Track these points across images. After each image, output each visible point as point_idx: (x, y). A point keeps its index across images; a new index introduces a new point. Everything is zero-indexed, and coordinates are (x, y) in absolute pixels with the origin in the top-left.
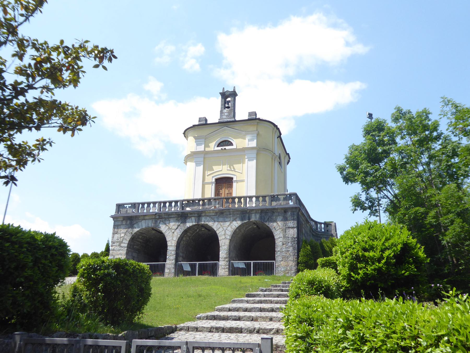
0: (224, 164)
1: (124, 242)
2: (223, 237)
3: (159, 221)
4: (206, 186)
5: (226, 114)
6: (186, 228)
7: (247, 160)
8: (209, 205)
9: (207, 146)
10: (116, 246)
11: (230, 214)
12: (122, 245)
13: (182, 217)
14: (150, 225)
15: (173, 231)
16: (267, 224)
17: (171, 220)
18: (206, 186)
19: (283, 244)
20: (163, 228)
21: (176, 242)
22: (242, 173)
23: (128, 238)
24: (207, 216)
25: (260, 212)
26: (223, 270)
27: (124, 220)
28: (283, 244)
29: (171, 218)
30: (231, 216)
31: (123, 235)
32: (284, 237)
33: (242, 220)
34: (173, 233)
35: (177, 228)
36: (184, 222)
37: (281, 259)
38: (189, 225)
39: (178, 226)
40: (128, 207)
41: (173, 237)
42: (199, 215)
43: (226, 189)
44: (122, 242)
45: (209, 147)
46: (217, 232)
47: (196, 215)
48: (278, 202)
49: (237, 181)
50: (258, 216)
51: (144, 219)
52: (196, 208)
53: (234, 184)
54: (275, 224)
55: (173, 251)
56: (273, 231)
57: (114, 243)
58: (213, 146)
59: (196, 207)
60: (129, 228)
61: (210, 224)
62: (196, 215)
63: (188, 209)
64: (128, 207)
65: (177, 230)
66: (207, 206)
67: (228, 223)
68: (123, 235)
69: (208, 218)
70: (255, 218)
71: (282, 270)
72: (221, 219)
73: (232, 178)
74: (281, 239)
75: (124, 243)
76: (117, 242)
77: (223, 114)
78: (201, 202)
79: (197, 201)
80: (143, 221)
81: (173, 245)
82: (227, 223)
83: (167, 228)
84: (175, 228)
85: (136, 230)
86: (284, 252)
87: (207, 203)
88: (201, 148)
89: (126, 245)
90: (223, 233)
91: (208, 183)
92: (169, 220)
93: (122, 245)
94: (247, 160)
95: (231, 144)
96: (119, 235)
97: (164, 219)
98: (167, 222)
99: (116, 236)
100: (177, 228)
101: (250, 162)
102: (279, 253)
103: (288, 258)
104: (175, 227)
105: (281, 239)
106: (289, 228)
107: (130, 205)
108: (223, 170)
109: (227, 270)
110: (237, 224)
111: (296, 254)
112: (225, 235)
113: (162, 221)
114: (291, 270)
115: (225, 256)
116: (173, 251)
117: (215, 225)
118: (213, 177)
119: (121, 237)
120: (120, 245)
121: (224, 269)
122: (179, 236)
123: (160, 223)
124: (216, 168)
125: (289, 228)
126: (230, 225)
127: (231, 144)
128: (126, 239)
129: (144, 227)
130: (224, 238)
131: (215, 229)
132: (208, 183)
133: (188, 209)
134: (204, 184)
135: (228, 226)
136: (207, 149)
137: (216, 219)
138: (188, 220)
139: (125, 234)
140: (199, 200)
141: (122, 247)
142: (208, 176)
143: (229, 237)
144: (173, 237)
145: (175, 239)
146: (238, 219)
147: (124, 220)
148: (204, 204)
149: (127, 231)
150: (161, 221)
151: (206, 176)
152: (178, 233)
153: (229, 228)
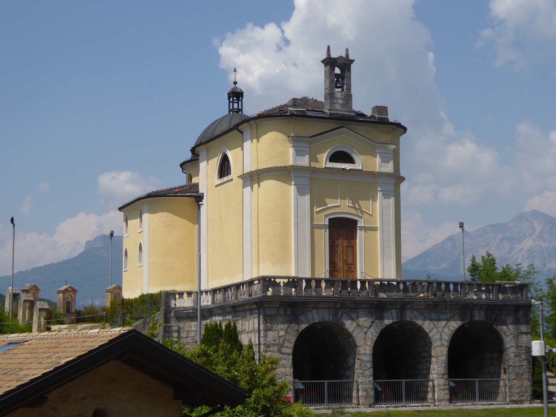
0: (343, 198)
1: (286, 344)
2: (439, 343)
3: (340, 313)
4: (316, 231)
5: (340, 101)
6: (385, 326)
7: (379, 194)
8: (413, 292)
9: (313, 159)
10: (273, 351)
11: (446, 309)
12: (284, 350)
13: (377, 309)
14: (327, 318)
15: (365, 330)
16: (495, 326)
17: (361, 312)
18: (316, 231)
19: (516, 356)
20: (349, 325)
21: (372, 348)
22: (371, 215)
23: (293, 338)
24: (415, 309)
25: (485, 308)
26: (443, 392)
27: (281, 306)
28: (516, 356)
29: (360, 308)
30: (448, 311)
31: (282, 333)
32: (517, 346)
33: (462, 319)
34: (366, 333)
35: (371, 326)
36: (381, 318)
37: (514, 377)
38: (387, 322)
39: (373, 322)
40: (282, 284)
41: (365, 339)
42: (402, 306)
43: (345, 241)
44: (282, 346)
45: (317, 161)
46: (431, 335)
47: (398, 307)
48: (505, 295)
49: (366, 229)
50: (483, 314)
51: (316, 308)
52: (395, 295)
53: (360, 234)
54: (505, 327)
55: (369, 362)
56: (503, 336)
57: (269, 347)
58: (323, 161)
59: (395, 293)
60: (291, 322)
61: (420, 322)
62: (398, 307)
63: (382, 295)
64: (282, 284)
65: (372, 330)
66: (411, 293)
67: (443, 323)
68: (282, 333)
69: (415, 312)
70: (479, 316)
71: (517, 391)
72: (434, 315)
73: (355, 222)
74: (512, 350)
75: (287, 347)
76: (275, 345)
77: (335, 101)
78: (401, 286)
79: (395, 283)
80: (314, 312)
81: (368, 352)
82: (442, 322)
83: (355, 324)
84: (368, 325)
85: (303, 326)
86: (517, 368)
87: (410, 288)
88: (305, 161)
89: (290, 351)
90: (438, 336)
91: (320, 227)
92: (357, 312)
93: (284, 350)
94: (379, 194)
95: (352, 161)
96: (276, 333)
97: (348, 310)
98: (354, 316)
99: (271, 334)
100: (371, 326)
101: (386, 201)
102: (511, 368)
103: (522, 375)
104: (367, 324)
105: (512, 350)
106: (522, 333)
107: (286, 281)
108: (341, 207)
109: (447, 392)
110: (455, 325)
111: (531, 371)
112: (441, 339)
113: (346, 313)
114: (526, 392)
115: (443, 372)
116: (369, 362)
117: (427, 325)
118: (326, 216)
119: (279, 337)
120: (280, 351)
121: (443, 390)
122: (375, 338)
123: (342, 315)
124: (331, 203)
125: (522, 333)
126: (446, 324)
127: (352, 161)
128: (289, 341)
129: (316, 321)
130: (440, 344)
131: (427, 331)
132: (320, 227)
133: (382, 295)
134: (313, 227)
135: (445, 326)
136: (314, 165)
137: (427, 315)
138: (386, 314)
139: (287, 332)
140: (398, 283)
141: (284, 354)
142: (317, 212)
143: (446, 344)
144: (365, 339)
145: (369, 343)
146: (456, 317)
147: (281, 306)
148: (406, 290)
149: (288, 327)
150: (343, 313)
151: (315, 214)
152: (373, 334)
153: (446, 330)
